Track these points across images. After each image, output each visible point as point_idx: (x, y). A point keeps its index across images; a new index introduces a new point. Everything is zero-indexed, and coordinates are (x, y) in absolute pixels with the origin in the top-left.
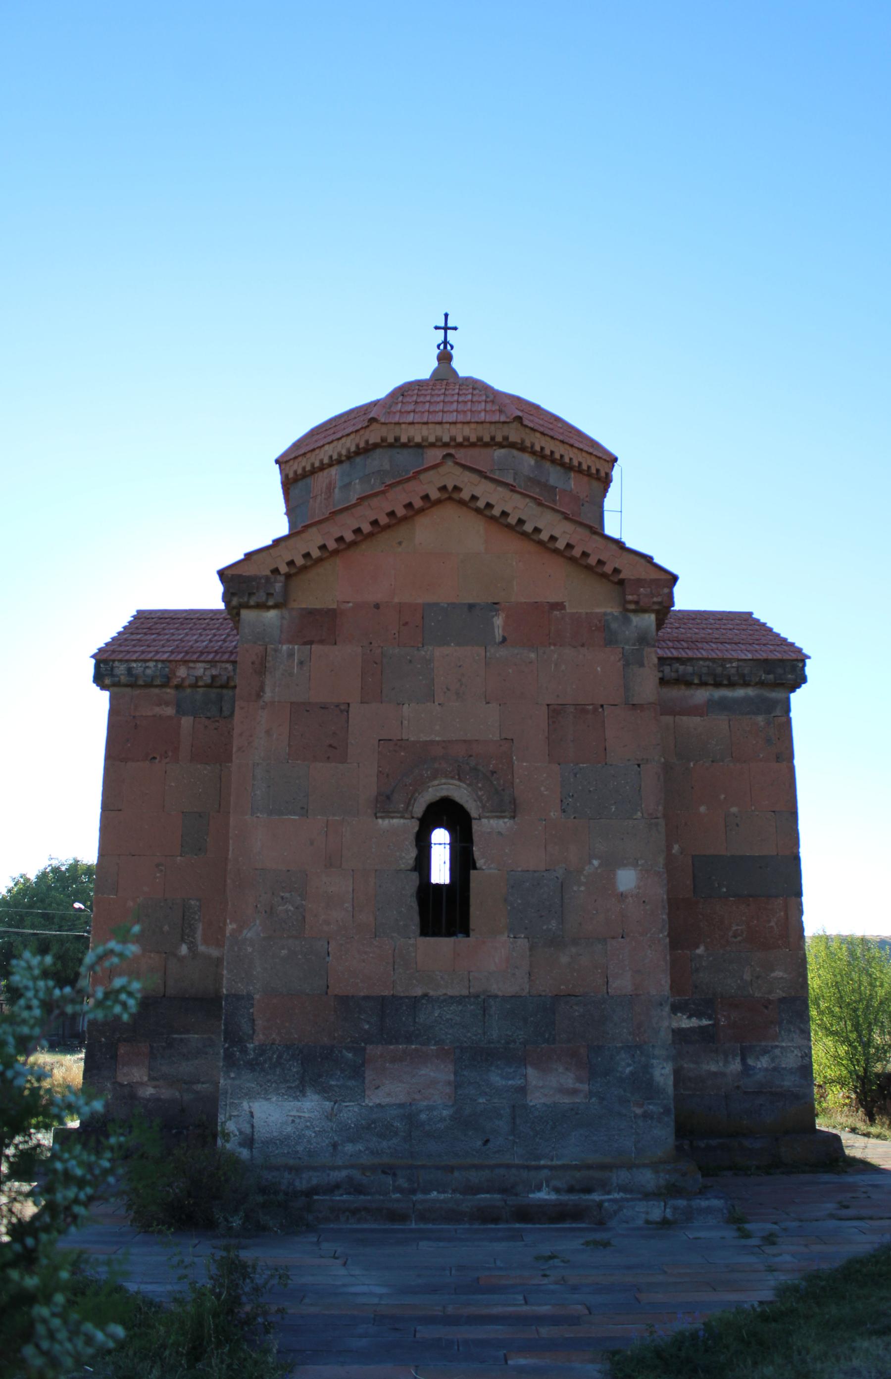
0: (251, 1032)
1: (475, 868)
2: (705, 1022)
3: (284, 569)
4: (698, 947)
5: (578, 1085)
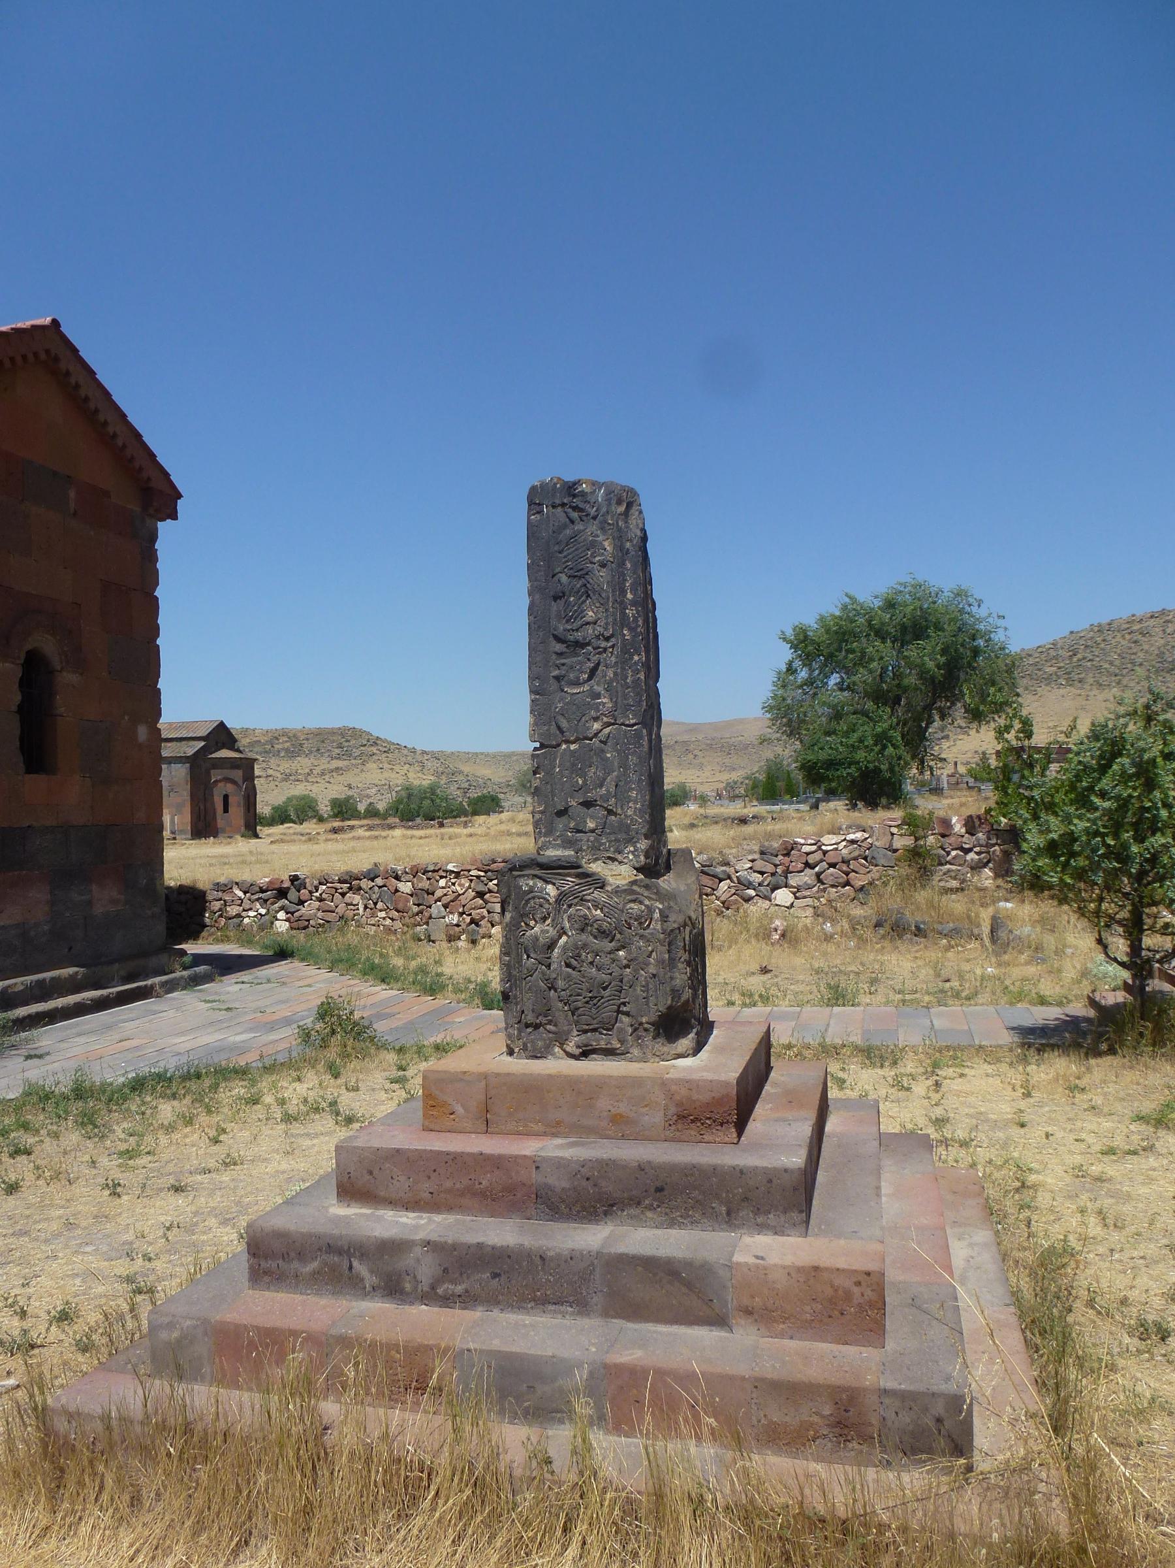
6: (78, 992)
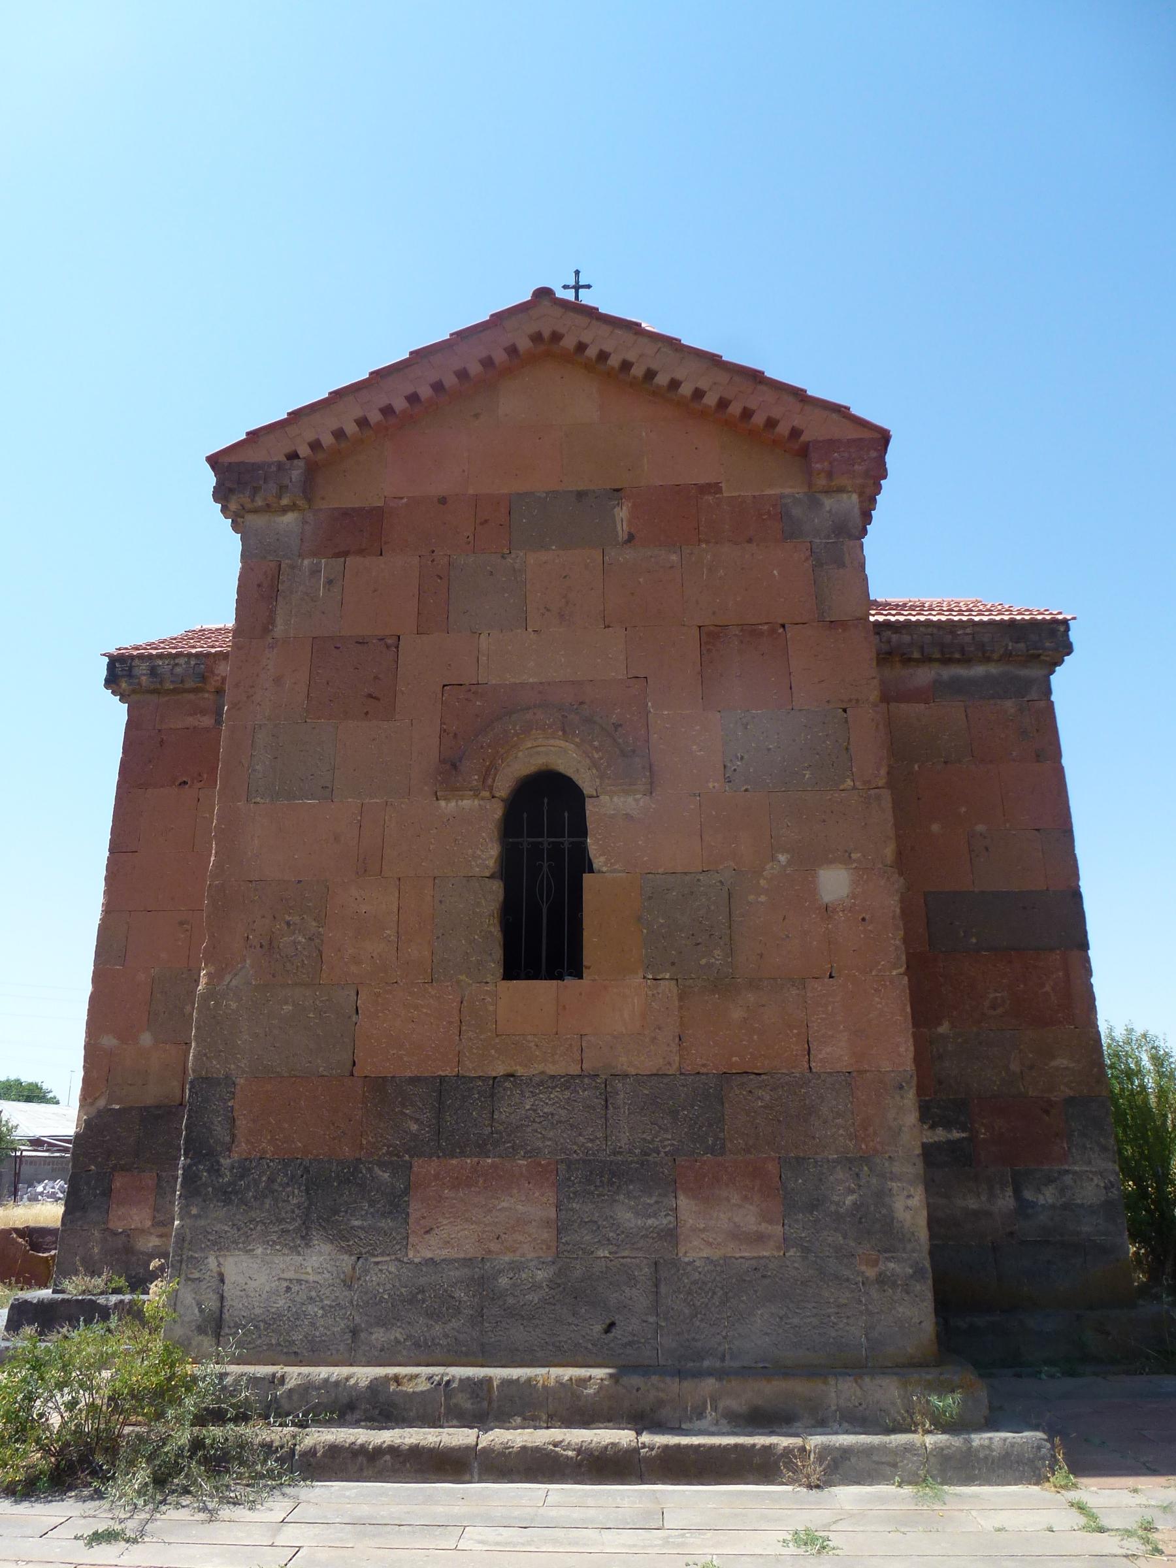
0: (228, 1139)
1: (591, 871)
2: (956, 1135)
3: (304, 451)
4: (940, 1024)
5: (764, 1227)
6: (586, 1424)
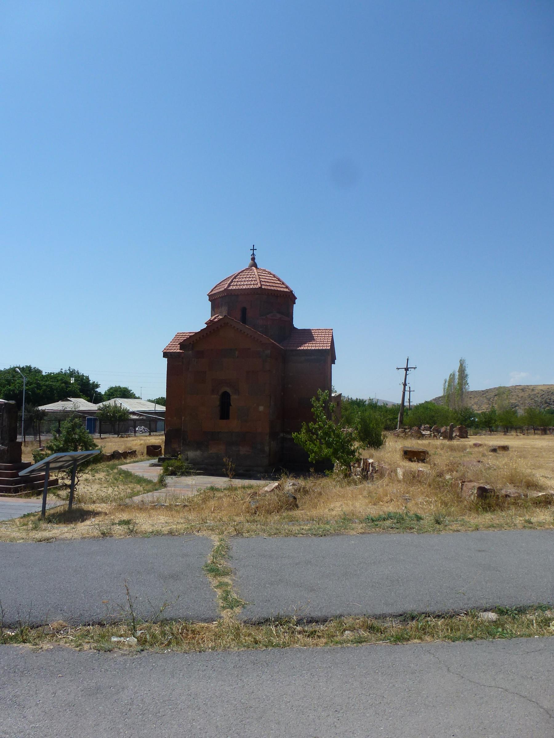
3: (192, 343)
